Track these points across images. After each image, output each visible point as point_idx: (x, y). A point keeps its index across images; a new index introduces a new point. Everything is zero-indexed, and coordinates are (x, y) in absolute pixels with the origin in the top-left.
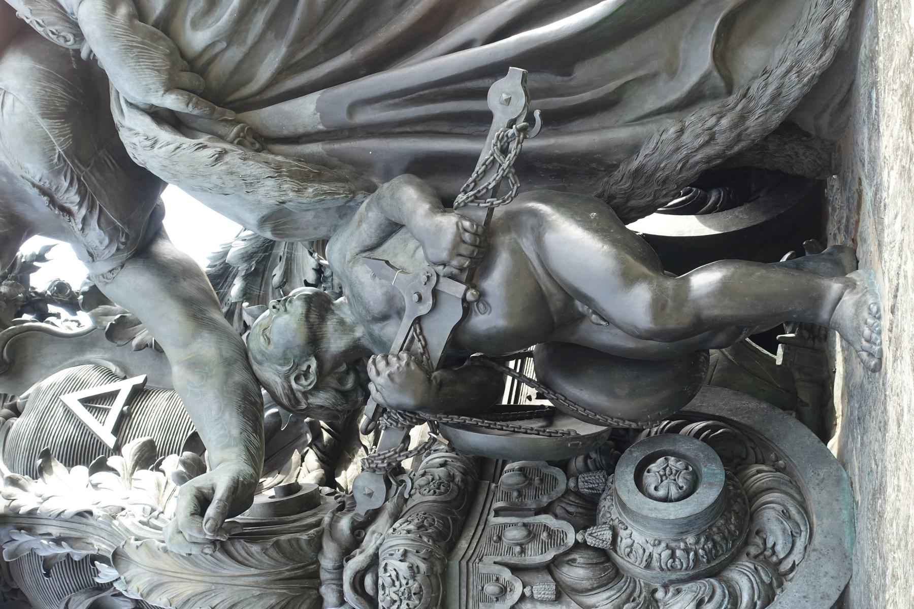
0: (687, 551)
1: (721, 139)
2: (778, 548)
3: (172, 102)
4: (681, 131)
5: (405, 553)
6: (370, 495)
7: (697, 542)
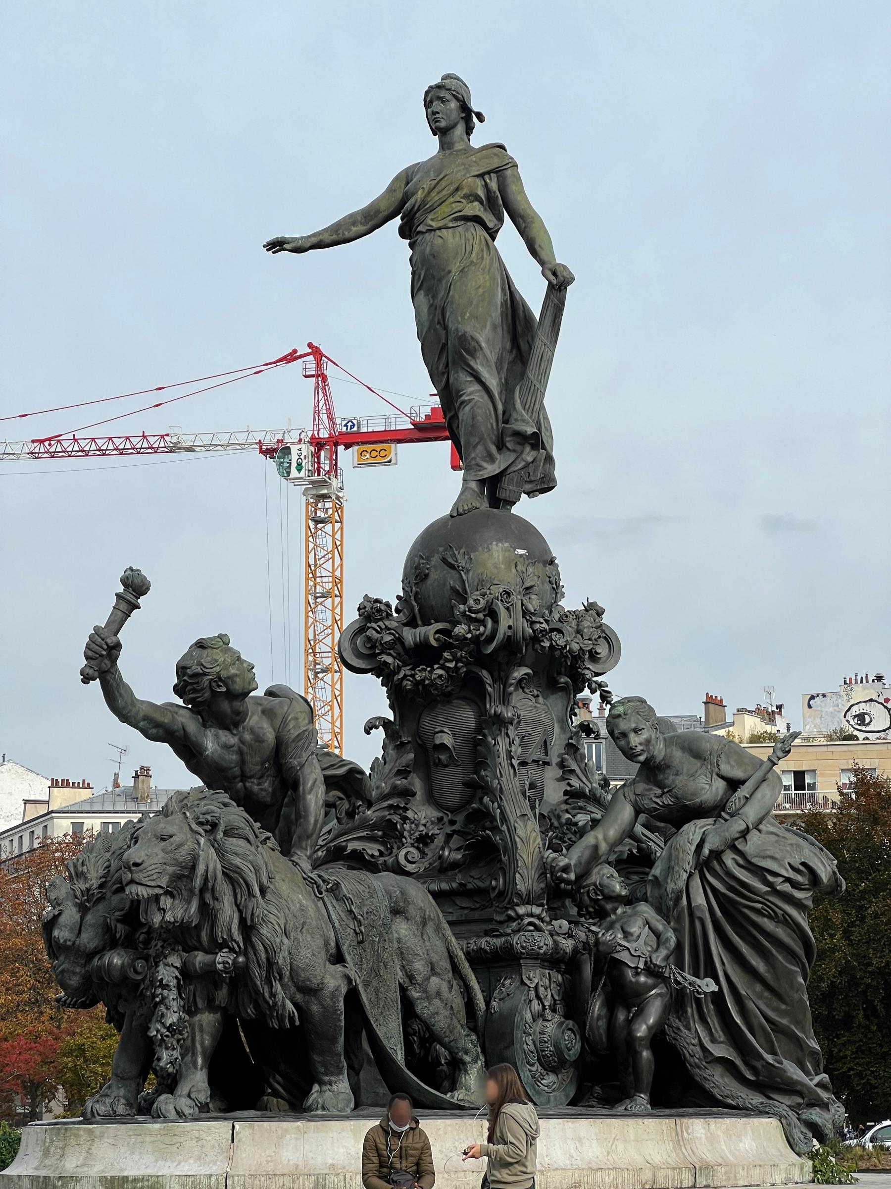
0: (548, 1047)
1: (692, 1060)
2: (544, 1081)
3: (706, 851)
4: (694, 1045)
5: (547, 945)
6: (560, 927)
7: (550, 1051)
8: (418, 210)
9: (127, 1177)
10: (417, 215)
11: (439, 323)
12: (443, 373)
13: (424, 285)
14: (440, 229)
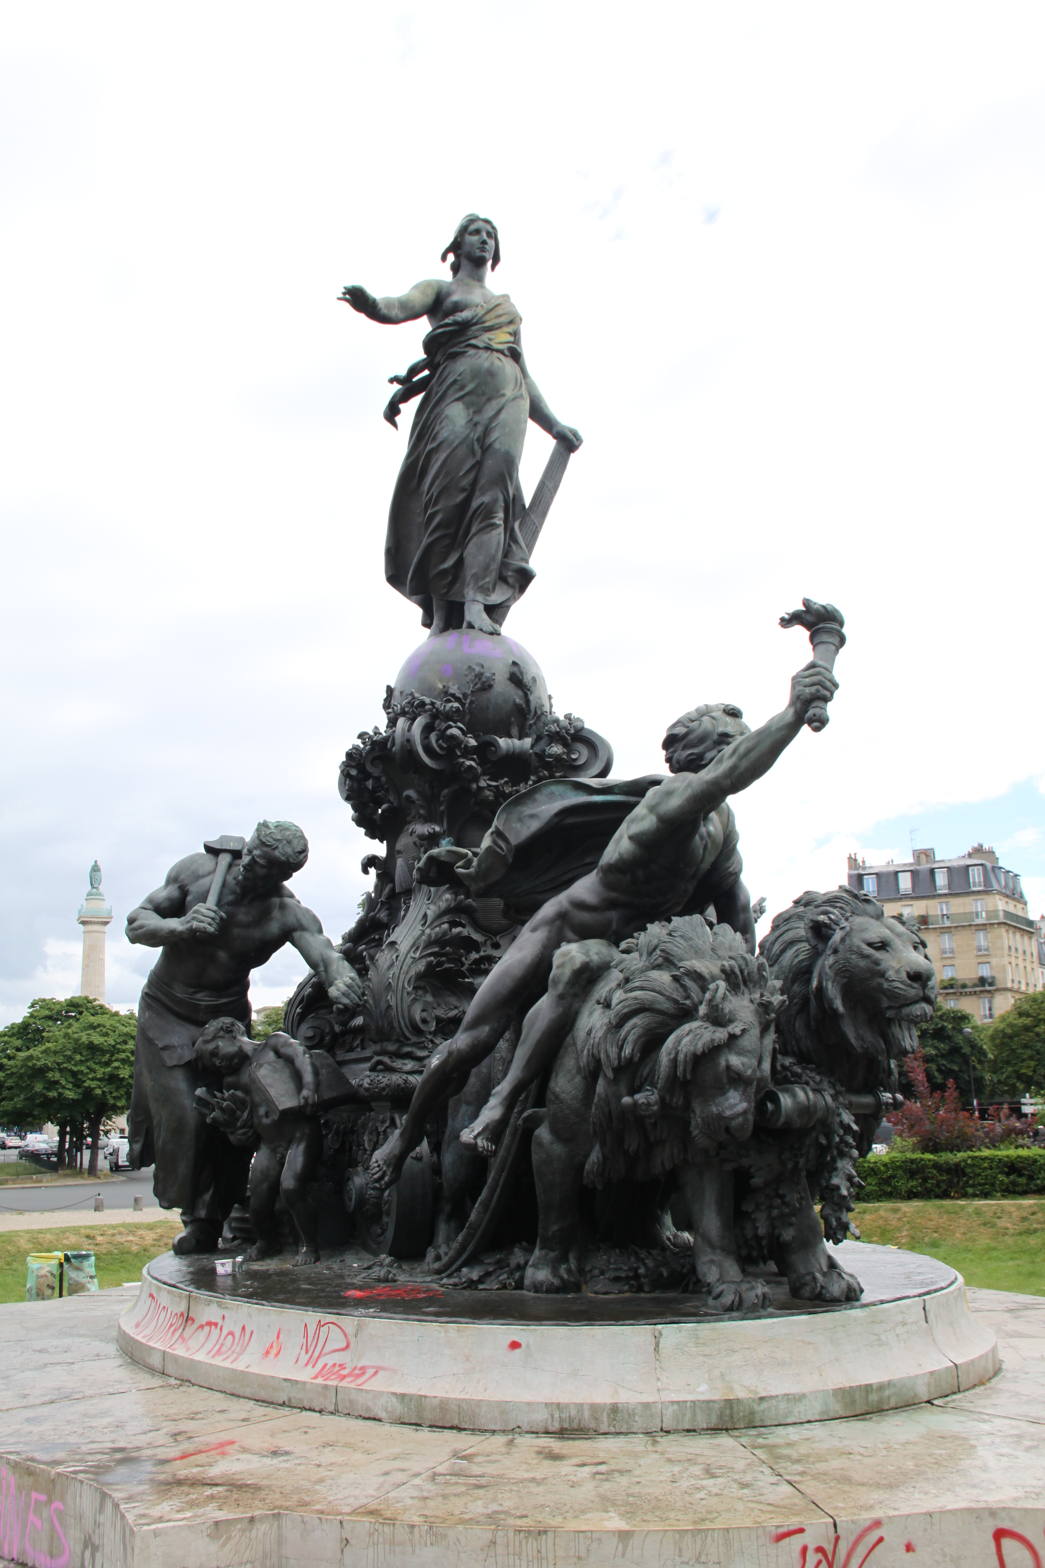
8: (475, 324)
9: (871, 1385)
10: (474, 328)
11: (478, 440)
12: (463, 490)
13: (467, 399)
14: (498, 351)
